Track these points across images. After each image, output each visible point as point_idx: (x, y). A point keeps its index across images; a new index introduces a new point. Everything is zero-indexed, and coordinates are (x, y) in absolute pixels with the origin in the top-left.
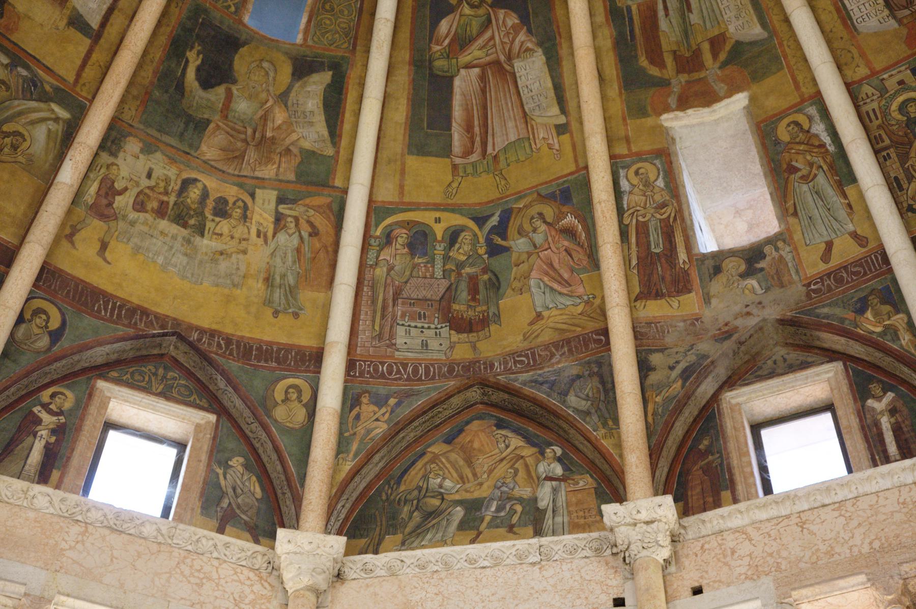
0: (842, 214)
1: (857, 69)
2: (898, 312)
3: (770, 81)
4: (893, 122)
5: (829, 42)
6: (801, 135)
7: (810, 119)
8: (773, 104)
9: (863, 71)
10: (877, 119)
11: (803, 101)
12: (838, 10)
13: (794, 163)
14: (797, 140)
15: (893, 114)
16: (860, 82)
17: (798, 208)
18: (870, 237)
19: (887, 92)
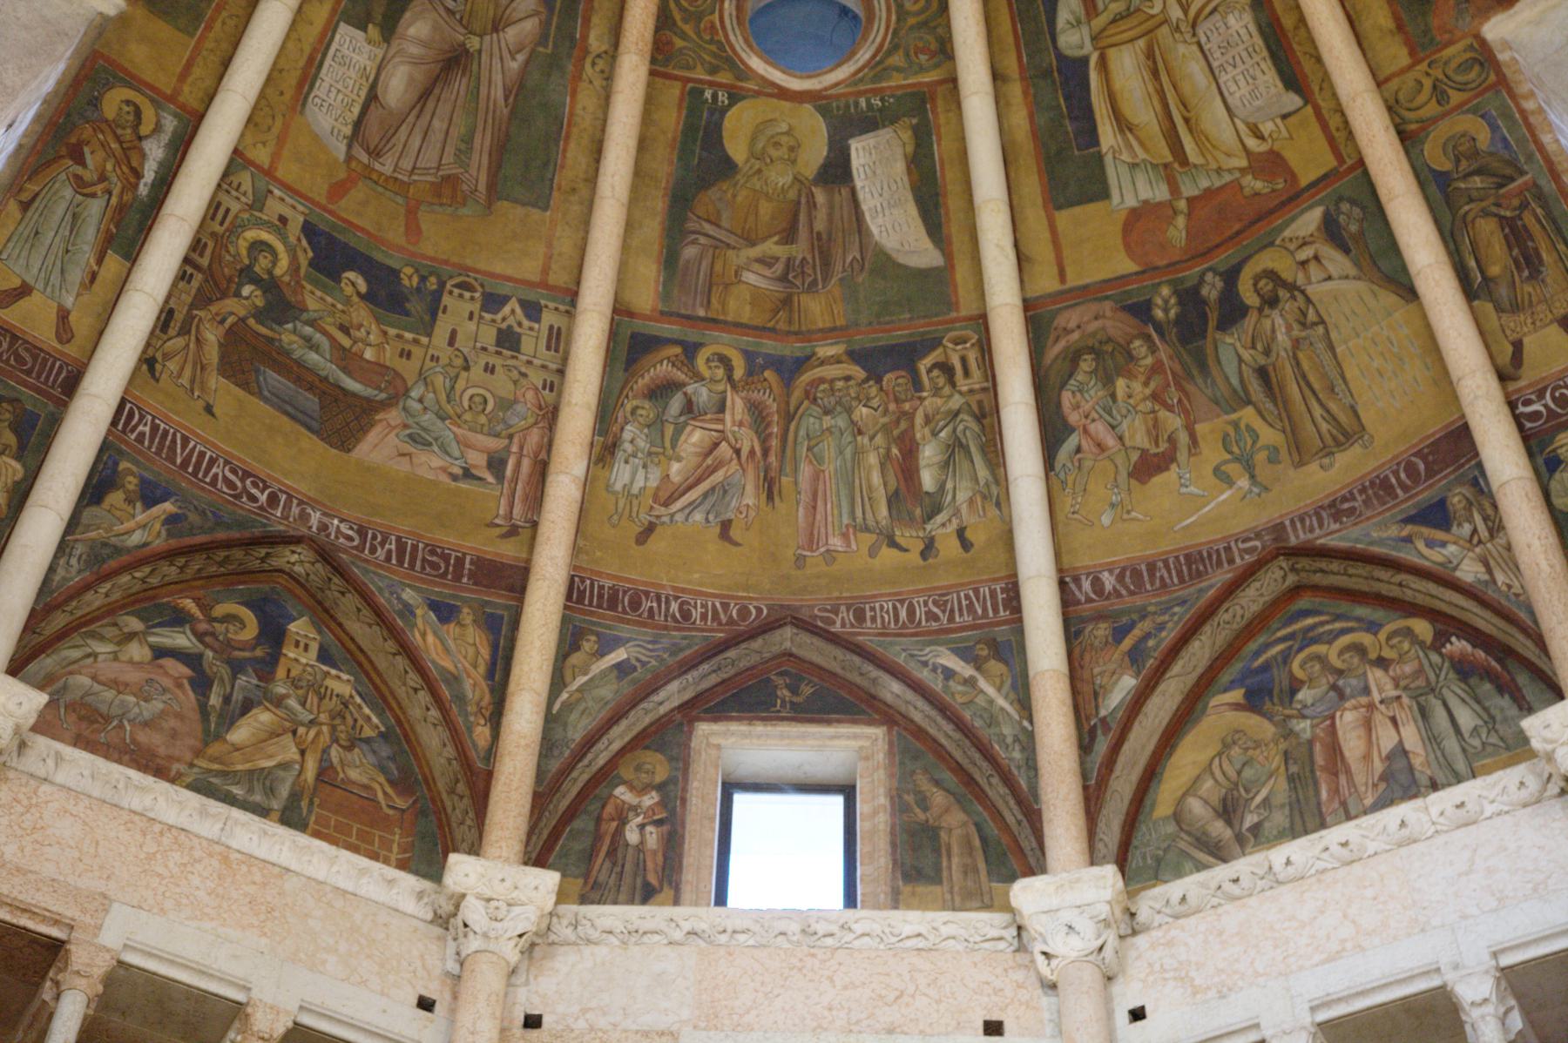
0: (76, 275)
1: (259, 146)
2: (18, 458)
3: (162, 30)
4: (232, 249)
5: (269, 80)
6: (129, 131)
7: (158, 128)
8: (137, 56)
9: (262, 155)
10: (221, 224)
11: (171, 99)
12: (311, 59)
13: (86, 150)
14: (119, 132)
15: (241, 242)
16: (251, 163)
17: (36, 204)
18: (78, 341)
19: (261, 211)
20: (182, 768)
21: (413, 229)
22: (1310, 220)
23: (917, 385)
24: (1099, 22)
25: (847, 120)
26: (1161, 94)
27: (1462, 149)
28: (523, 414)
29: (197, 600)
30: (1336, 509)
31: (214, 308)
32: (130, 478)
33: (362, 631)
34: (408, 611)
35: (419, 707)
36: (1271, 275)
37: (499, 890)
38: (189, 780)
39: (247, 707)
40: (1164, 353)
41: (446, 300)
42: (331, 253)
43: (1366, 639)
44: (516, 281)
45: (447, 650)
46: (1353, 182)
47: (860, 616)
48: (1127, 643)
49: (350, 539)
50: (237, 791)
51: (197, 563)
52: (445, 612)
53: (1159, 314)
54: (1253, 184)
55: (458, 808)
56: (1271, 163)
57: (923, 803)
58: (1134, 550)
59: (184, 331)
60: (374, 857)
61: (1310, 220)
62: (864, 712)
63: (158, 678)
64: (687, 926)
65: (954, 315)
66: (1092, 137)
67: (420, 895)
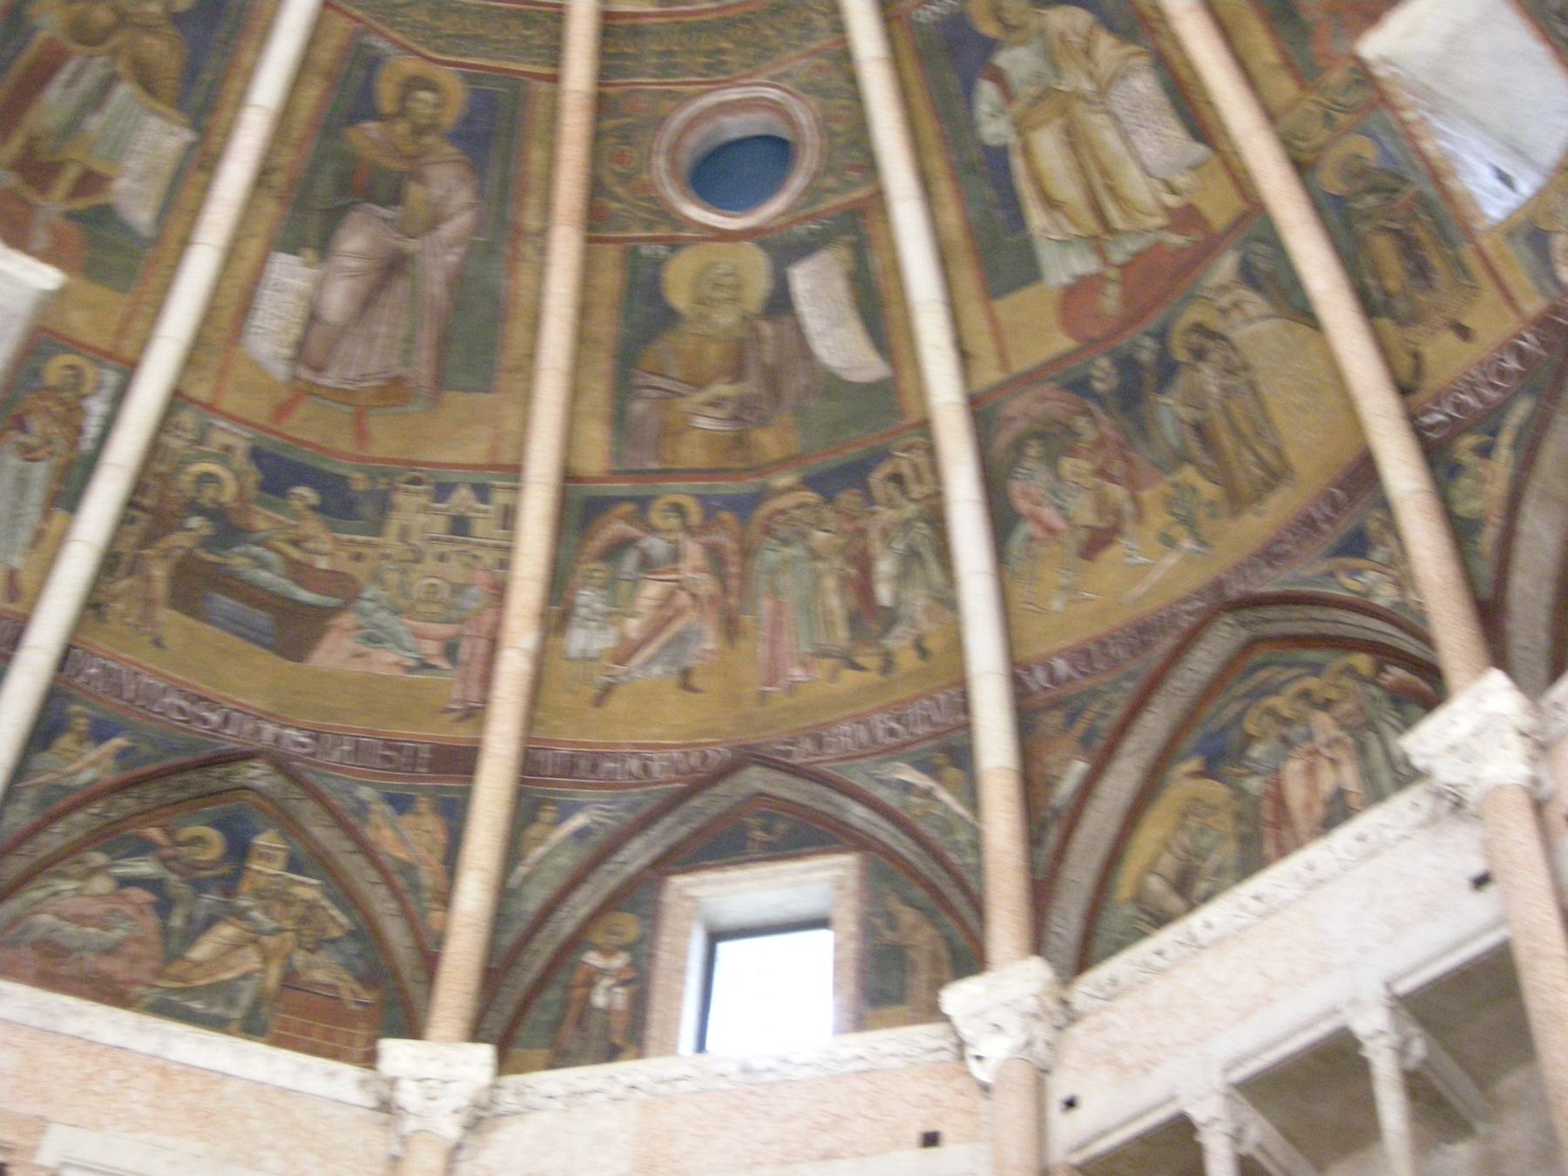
0: (24, 536)
3: (99, 293)
8: (78, 322)
9: (202, 391)
16: (192, 401)
20: (139, 989)
21: (361, 434)
22: (1226, 266)
23: (870, 499)
24: (1018, 108)
25: (786, 249)
26: (1082, 168)
27: (1357, 172)
28: (476, 597)
29: (164, 827)
30: (1270, 555)
31: (163, 544)
32: (82, 721)
33: (323, 833)
34: (363, 808)
35: (382, 904)
36: (1199, 328)
37: (432, 1070)
38: (148, 1000)
39: (210, 922)
40: (1107, 426)
41: (399, 498)
42: (277, 472)
43: (1311, 683)
44: (463, 466)
45: (403, 842)
46: (1255, 221)
47: (819, 742)
48: (1080, 727)
49: (303, 745)
50: (197, 1006)
51: (154, 792)
52: (400, 803)
53: (1099, 386)
54: (1176, 240)
55: (416, 990)
56: (1186, 217)
57: (892, 922)
58: (1085, 631)
59: (131, 572)
60: (335, 1055)
61: (1226, 266)
62: (836, 841)
63: (123, 907)
64: (626, 1080)
65: (904, 423)
66: (1018, 219)
67: (363, 1084)
